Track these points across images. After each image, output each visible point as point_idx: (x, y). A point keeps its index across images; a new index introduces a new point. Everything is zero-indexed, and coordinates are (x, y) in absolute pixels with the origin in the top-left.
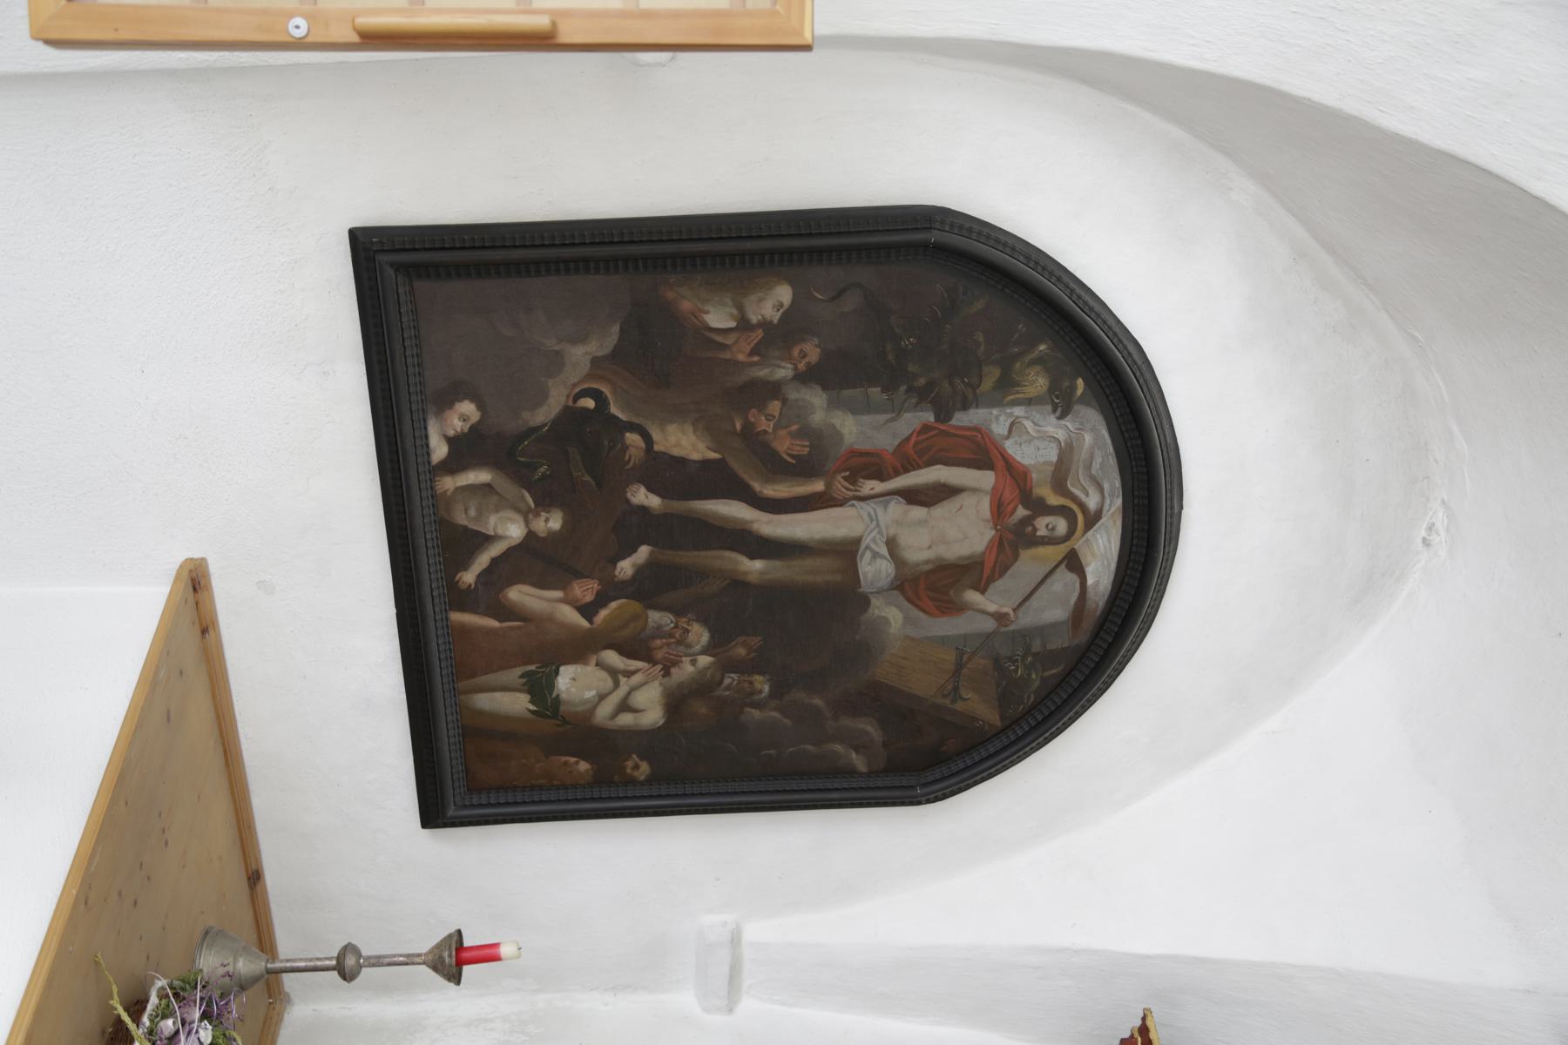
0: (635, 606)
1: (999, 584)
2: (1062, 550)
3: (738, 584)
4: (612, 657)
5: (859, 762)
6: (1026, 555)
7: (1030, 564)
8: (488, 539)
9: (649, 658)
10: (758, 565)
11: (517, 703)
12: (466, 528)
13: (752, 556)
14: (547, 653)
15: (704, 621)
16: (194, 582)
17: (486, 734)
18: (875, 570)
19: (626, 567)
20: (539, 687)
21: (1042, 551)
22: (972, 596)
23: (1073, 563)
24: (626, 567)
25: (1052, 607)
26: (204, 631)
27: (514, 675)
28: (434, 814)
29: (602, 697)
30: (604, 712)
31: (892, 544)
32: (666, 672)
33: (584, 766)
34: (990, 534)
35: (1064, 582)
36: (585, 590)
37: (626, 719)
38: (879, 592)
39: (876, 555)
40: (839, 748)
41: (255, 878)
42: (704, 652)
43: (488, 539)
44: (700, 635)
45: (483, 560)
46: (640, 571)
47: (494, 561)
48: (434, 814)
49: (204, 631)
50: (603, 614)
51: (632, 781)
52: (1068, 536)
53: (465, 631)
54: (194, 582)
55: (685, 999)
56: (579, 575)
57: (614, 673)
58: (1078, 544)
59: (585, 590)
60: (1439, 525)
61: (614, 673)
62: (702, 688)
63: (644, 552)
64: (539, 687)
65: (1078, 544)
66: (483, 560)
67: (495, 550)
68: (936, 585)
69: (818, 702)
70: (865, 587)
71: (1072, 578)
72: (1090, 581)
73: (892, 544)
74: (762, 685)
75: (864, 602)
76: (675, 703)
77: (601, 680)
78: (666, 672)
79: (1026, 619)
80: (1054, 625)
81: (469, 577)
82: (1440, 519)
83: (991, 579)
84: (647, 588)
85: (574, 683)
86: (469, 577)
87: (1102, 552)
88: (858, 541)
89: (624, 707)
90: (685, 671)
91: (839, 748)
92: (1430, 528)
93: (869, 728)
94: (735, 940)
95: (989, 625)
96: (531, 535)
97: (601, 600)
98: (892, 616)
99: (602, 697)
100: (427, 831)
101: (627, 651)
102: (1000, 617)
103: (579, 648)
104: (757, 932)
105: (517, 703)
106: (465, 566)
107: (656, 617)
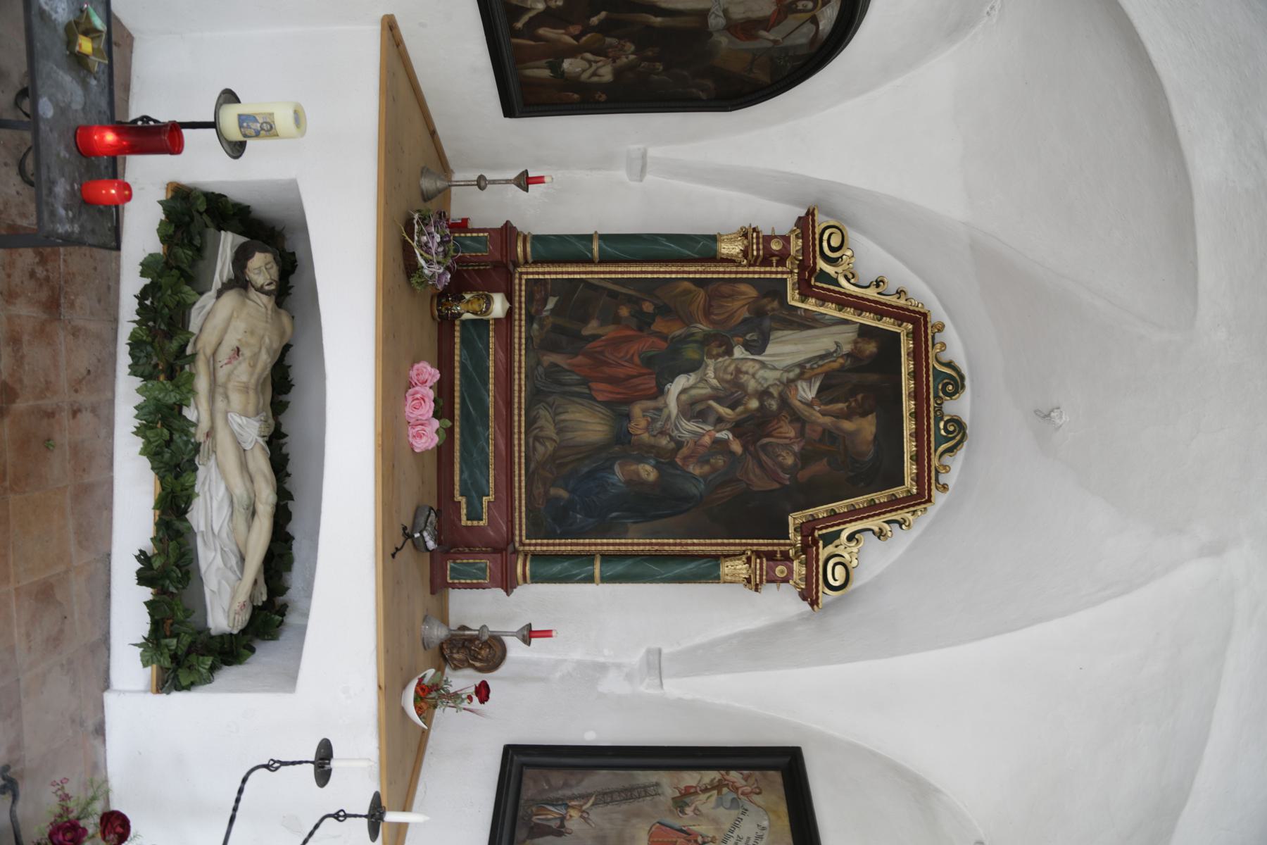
0: (599, 36)
1: (777, 28)
2: (808, 15)
3: (649, 27)
4: (589, 56)
5: (703, 96)
6: (790, 17)
7: (791, 21)
8: (528, 10)
9: (606, 56)
10: (659, 19)
11: (546, 73)
12: (517, 6)
13: (656, 16)
14: (558, 54)
15: (633, 42)
16: (390, 27)
17: (530, 85)
18: (716, 21)
19: (595, 20)
20: (555, 67)
21: (799, 15)
22: (763, 33)
23: (814, 21)
24: (595, 20)
25: (802, 37)
26: (398, 46)
27: (543, 62)
28: (510, 110)
29: (584, 71)
30: (585, 76)
31: (725, 12)
32: (614, 61)
33: (576, 96)
34: (774, 8)
35: (808, 29)
36: (576, 29)
37: (595, 79)
38: (718, 31)
39: (717, 16)
40: (694, 90)
41: (433, 133)
42: (633, 53)
43: (528, 10)
44: (630, 47)
45: (526, 18)
46: (601, 22)
47: (531, 19)
48: (509, 111)
49: (398, 46)
50: (584, 39)
51: (599, 102)
52: (815, 7)
53: (518, 46)
54: (390, 27)
55: (621, 174)
56: (572, 24)
57: (589, 62)
58: (818, 13)
59: (576, 29)
60: (997, 7)
61: (589, 62)
62: (631, 67)
63: (603, 14)
64: (555, 67)
65: (818, 13)
66: (526, 18)
67: (531, 14)
68: (746, 28)
69: (685, 73)
70: (711, 29)
71: (814, 28)
72: (821, 28)
73: (725, 12)
74: (660, 66)
75: (710, 35)
76: (618, 73)
77: (585, 64)
78: (614, 61)
79: (788, 42)
80: (801, 46)
81: (519, 25)
82: (998, 6)
83: (773, 26)
84: (604, 28)
85: (568, 65)
86: (519, 25)
87: (828, 17)
88: (709, 10)
89: (594, 74)
90: (624, 60)
91: (694, 90)
92: (992, 8)
93: (709, 83)
94: (644, 156)
95: (770, 45)
96: (548, 8)
97: (583, 34)
98: (724, 41)
99: (584, 71)
100: (508, 119)
101: (593, 53)
102: (775, 42)
103: (573, 52)
104: (653, 152)
105: (546, 73)
106: (518, 21)
107: (608, 40)
